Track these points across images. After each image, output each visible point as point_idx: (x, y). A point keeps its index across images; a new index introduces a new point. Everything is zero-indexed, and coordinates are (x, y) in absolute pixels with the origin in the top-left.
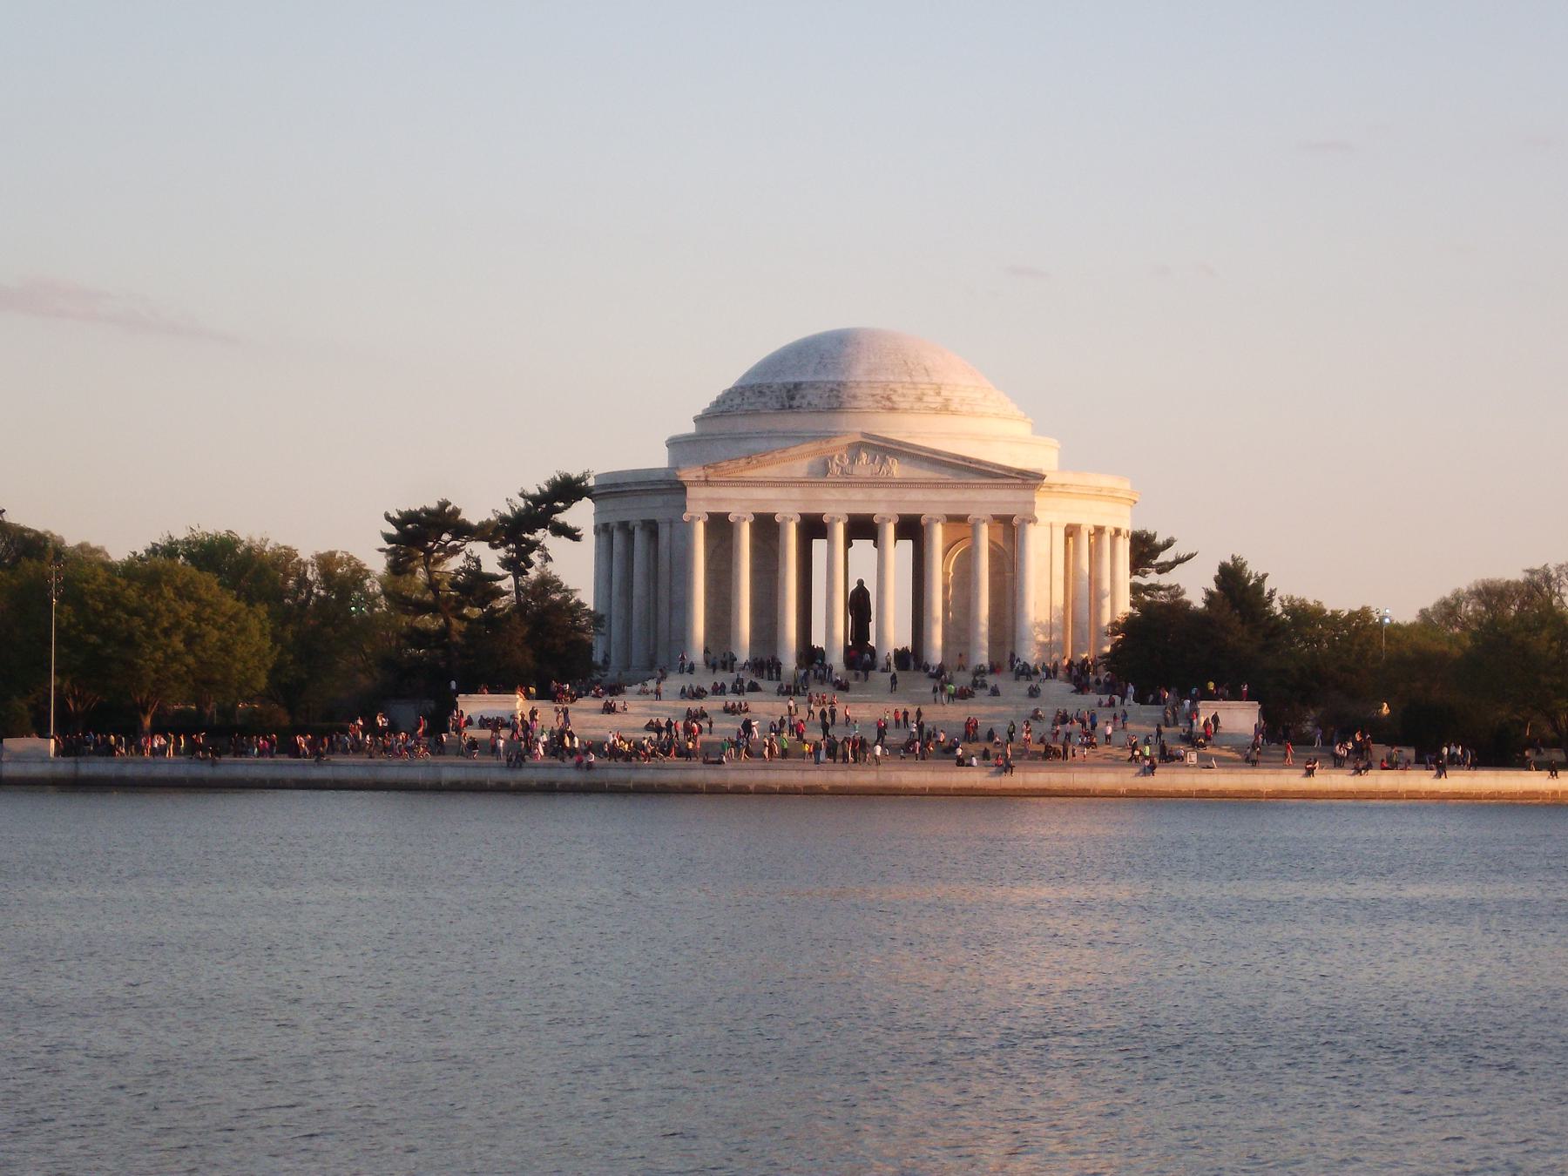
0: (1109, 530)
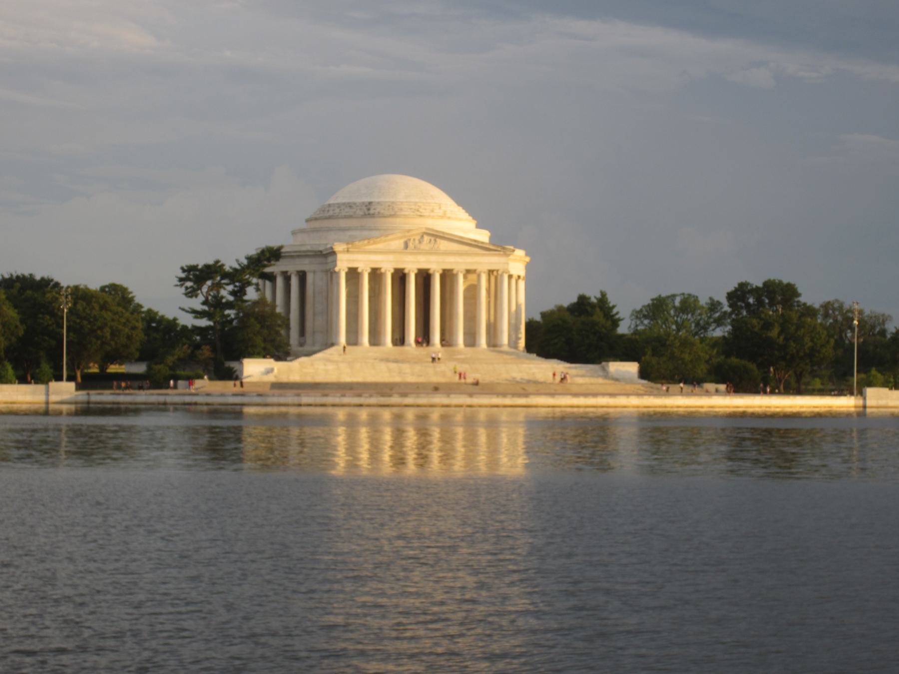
0: (515, 277)
